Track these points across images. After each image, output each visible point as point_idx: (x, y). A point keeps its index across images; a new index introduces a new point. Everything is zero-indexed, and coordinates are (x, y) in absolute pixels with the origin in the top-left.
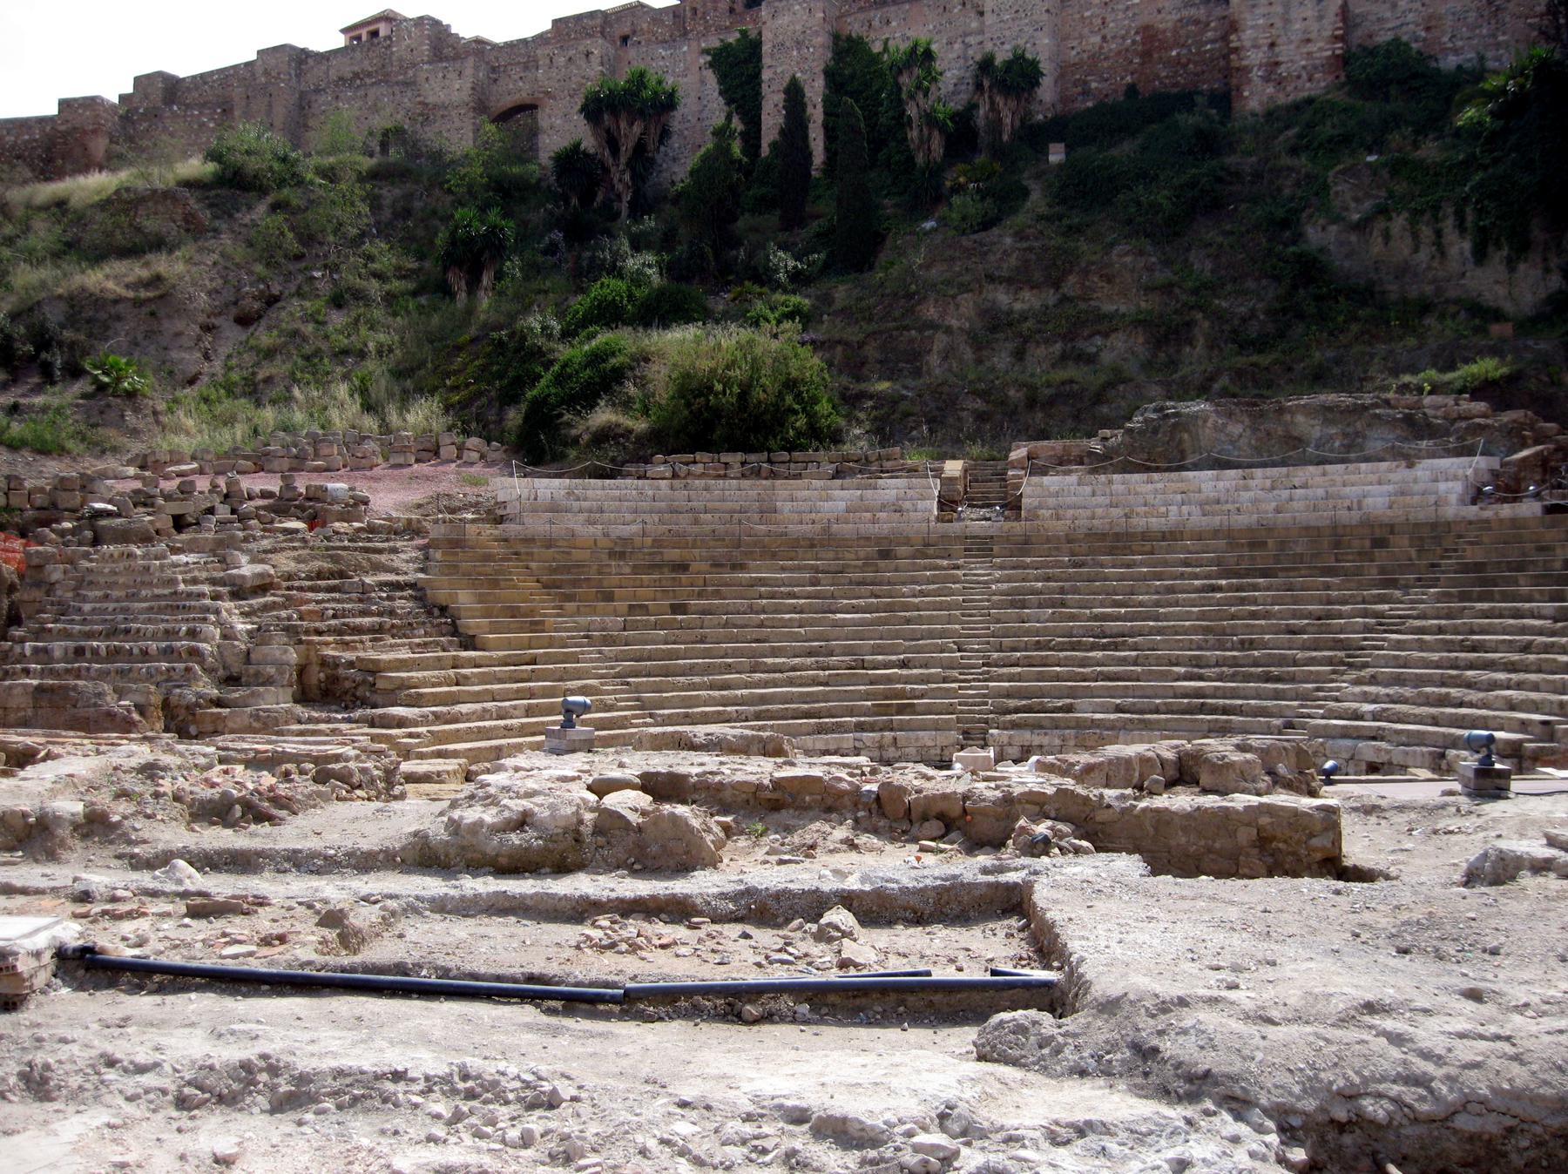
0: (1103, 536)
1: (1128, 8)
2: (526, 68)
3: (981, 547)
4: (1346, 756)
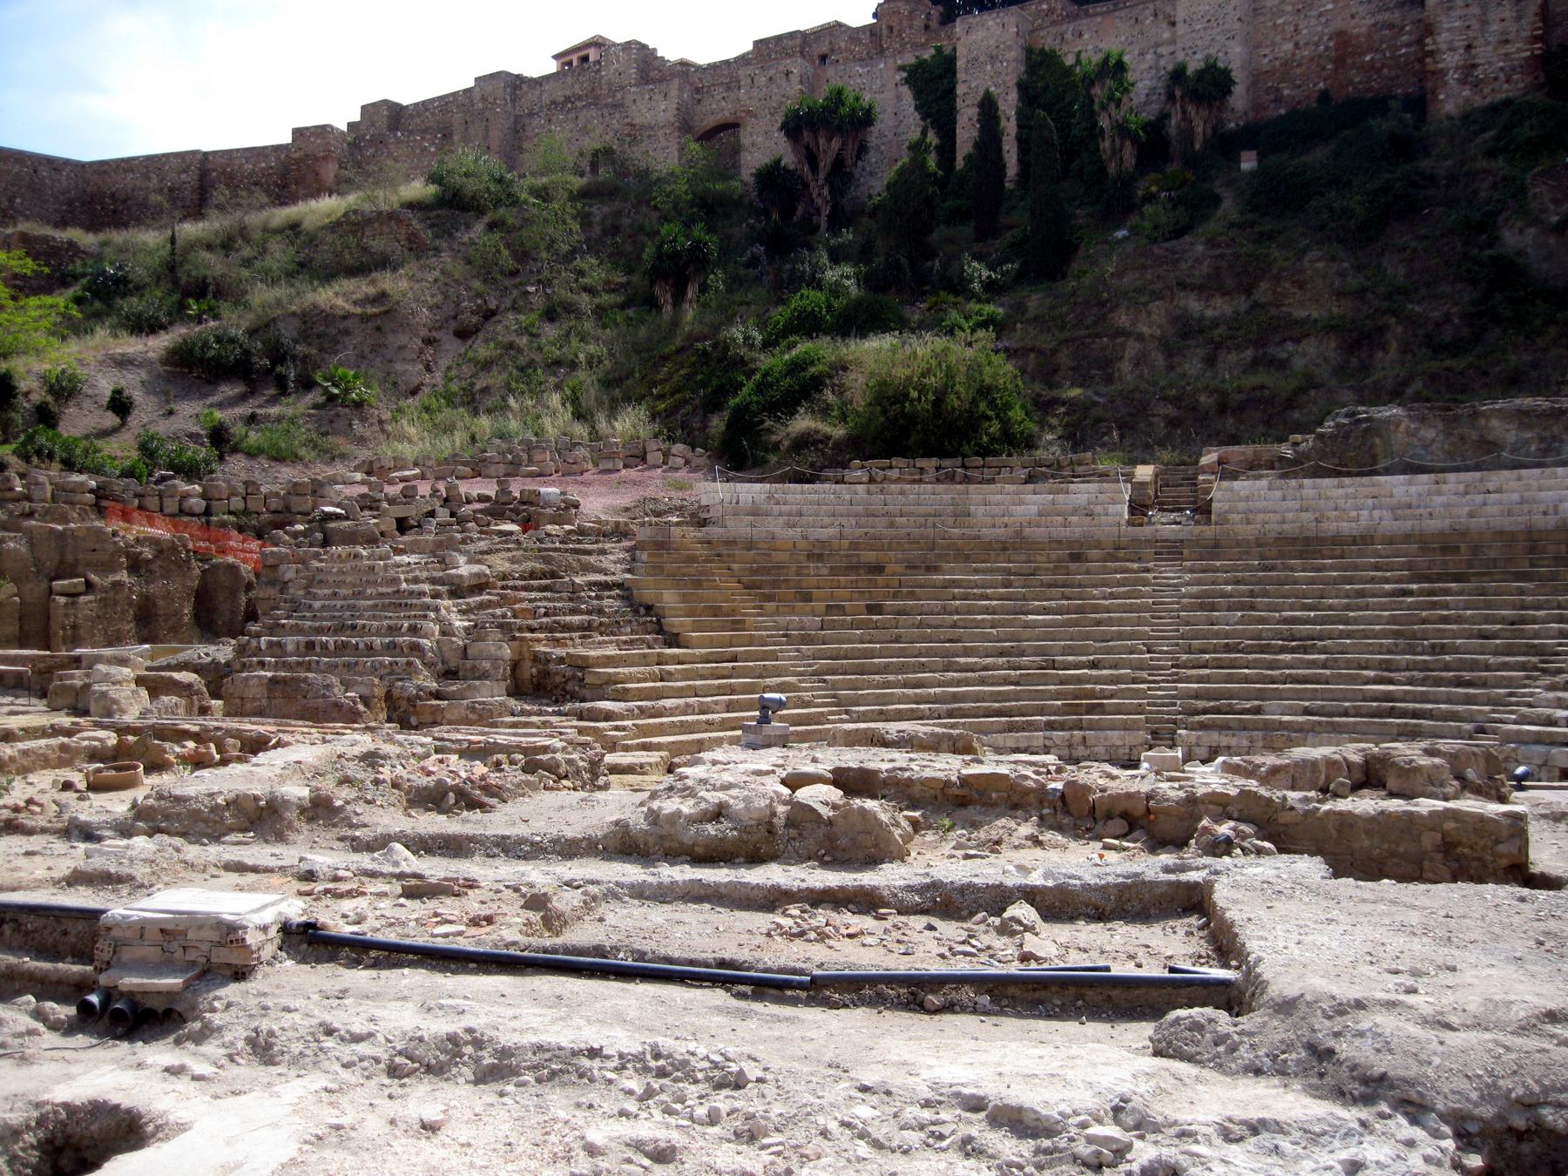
0: (1293, 540)
1: (1321, 15)
2: (729, 89)
3: (1172, 550)
4: (1539, 762)
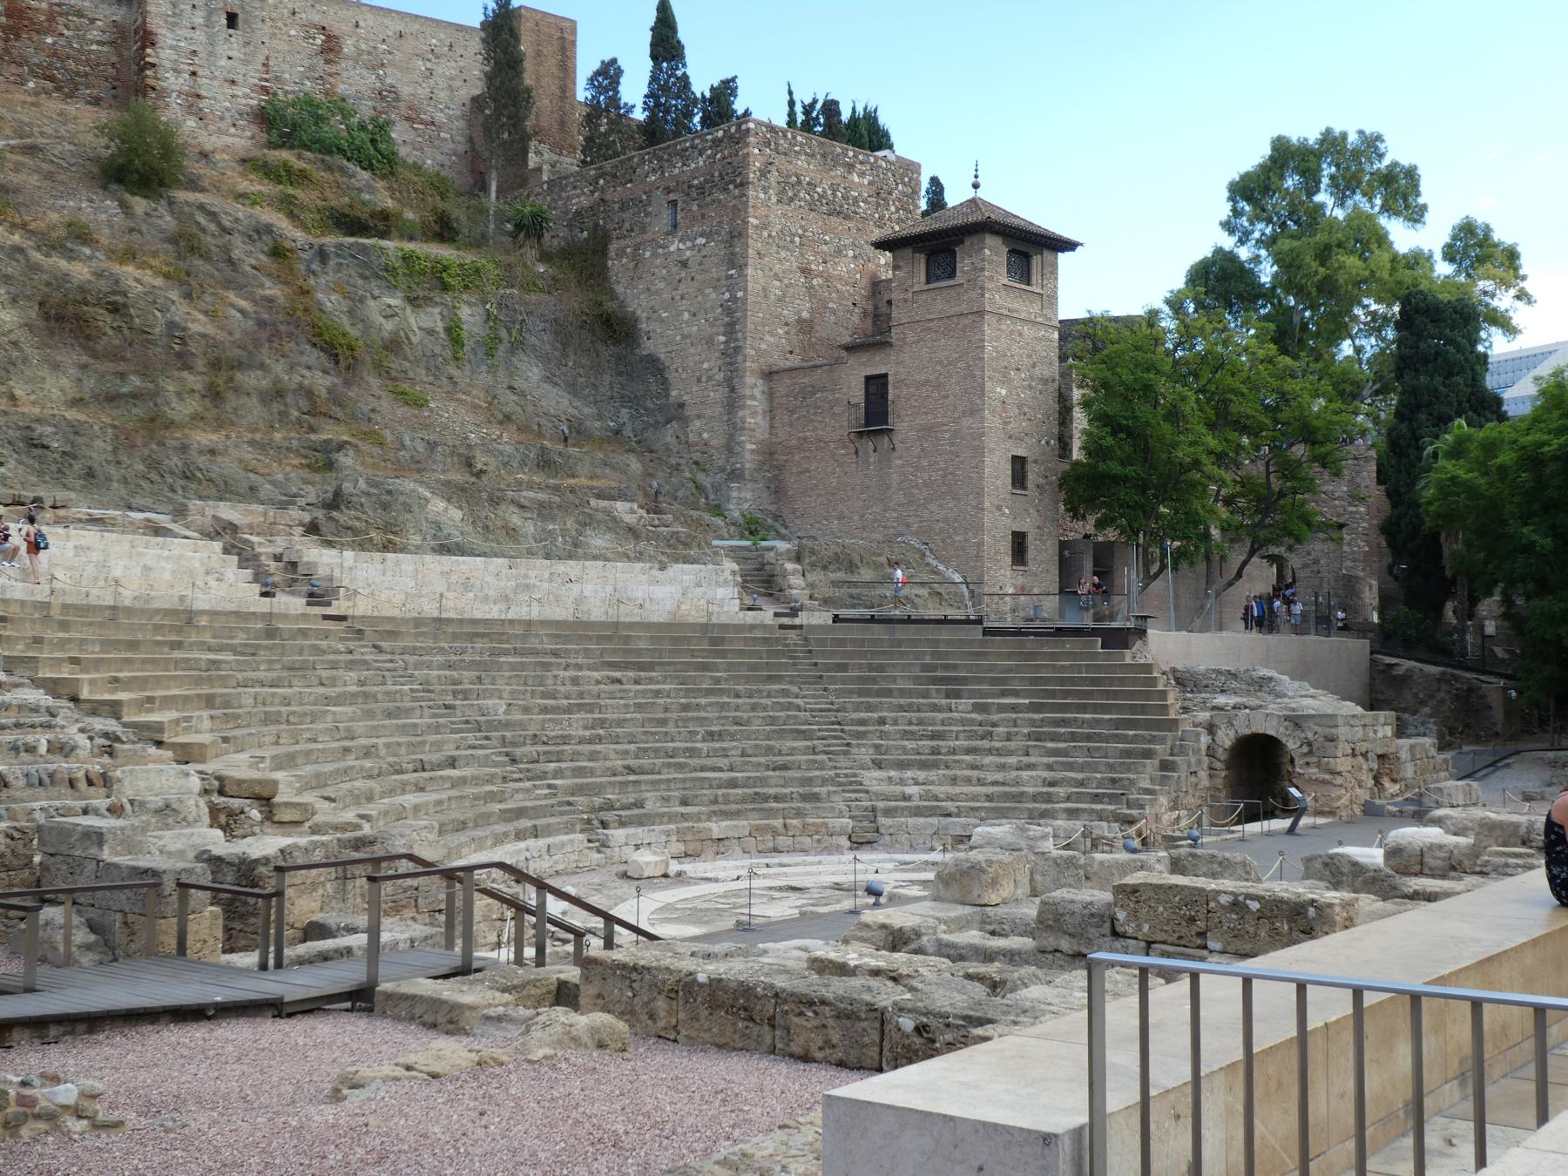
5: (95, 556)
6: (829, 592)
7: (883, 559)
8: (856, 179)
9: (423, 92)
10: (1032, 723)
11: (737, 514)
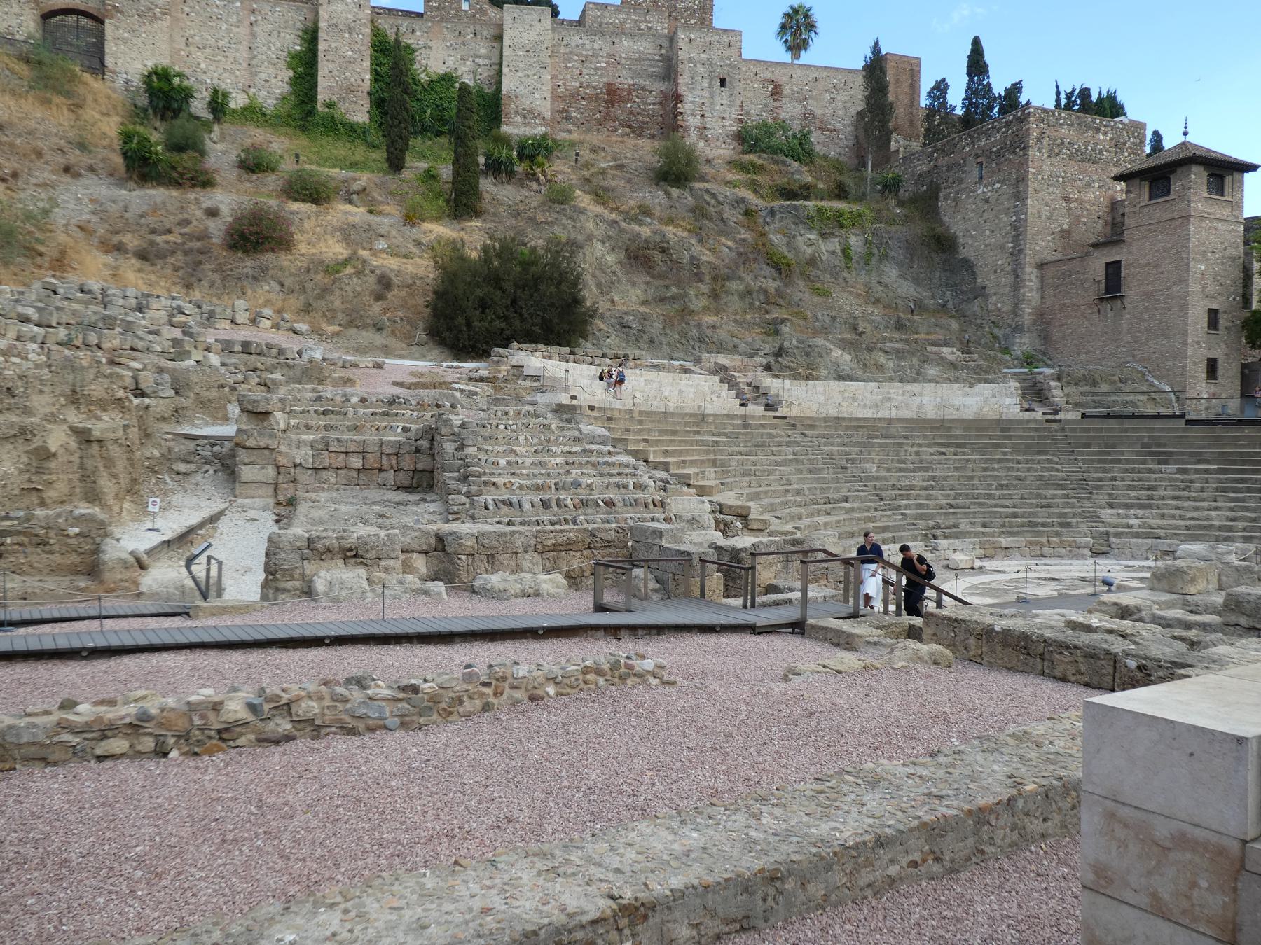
1: (596, 69)
5: (655, 385)
6: (1079, 399)
7: (1116, 378)
8: (1101, 137)
9: (829, 112)
10: (1220, 481)
11: (1019, 353)
